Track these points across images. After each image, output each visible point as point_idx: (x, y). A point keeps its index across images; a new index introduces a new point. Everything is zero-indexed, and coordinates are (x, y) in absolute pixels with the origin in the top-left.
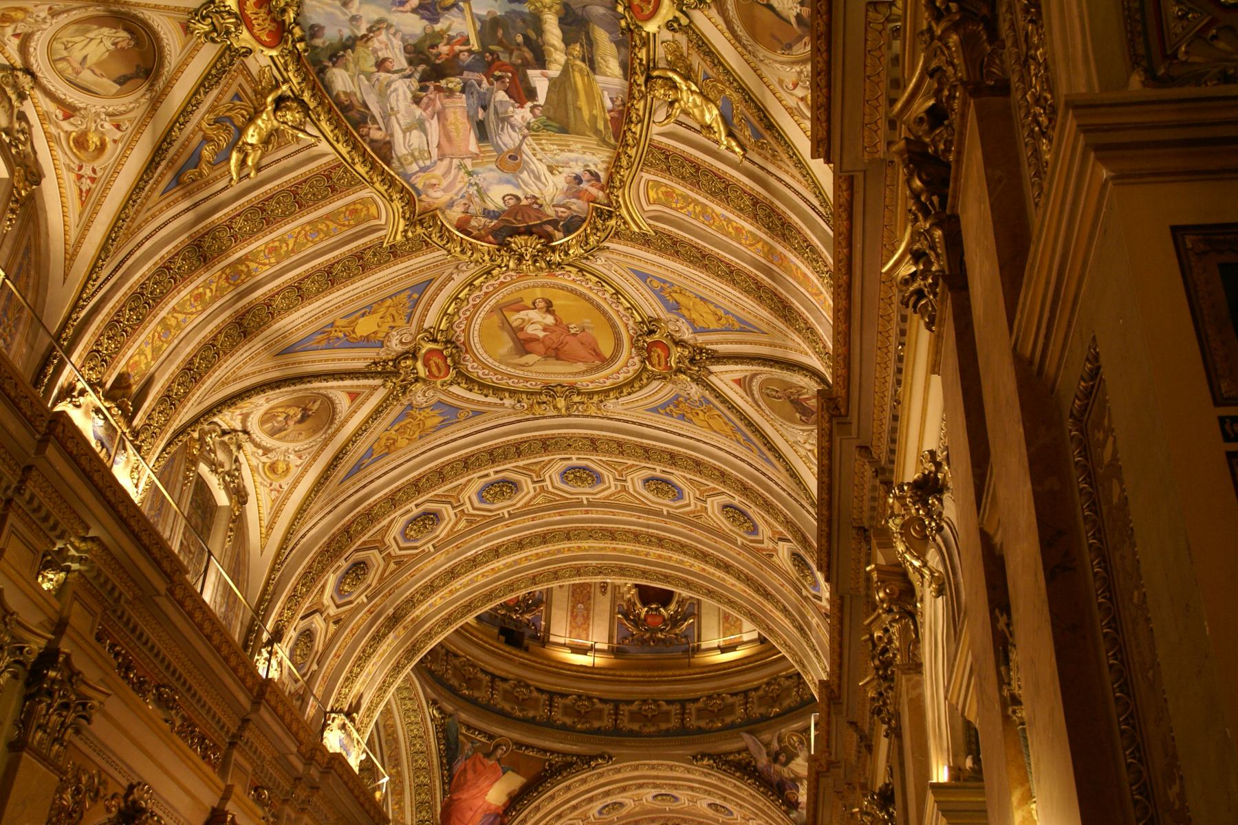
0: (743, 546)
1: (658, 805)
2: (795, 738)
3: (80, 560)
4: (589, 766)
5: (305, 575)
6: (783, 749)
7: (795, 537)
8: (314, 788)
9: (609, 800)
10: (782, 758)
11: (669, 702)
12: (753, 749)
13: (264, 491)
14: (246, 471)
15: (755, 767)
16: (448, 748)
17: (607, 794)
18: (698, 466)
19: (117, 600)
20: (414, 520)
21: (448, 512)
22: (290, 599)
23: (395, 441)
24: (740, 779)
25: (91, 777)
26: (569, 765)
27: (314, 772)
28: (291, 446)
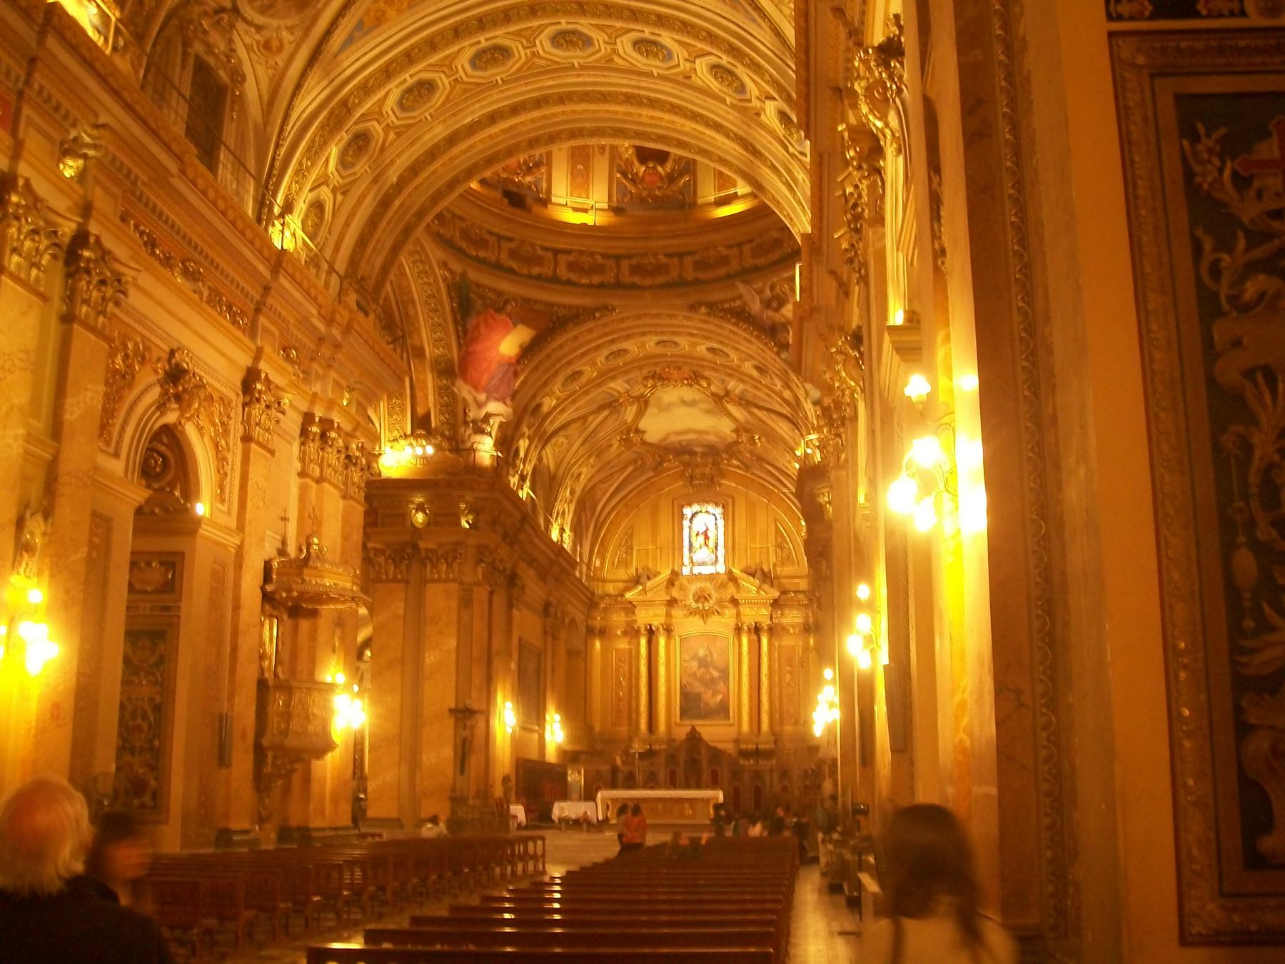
0: (733, 106)
1: (660, 350)
3: (95, 147)
4: (595, 318)
5: (309, 149)
6: (775, 297)
7: (781, 97)
8: (337, 346)
9: (615, 348)
10: (774, 304)
11: (668, 255)
12: (746, 297)
13: (261, 70)
14: (242, 52)
15: (749, 314)
16: (461, 305)
17: (613, 342)
18: (686, 27)
19: (134, 183)
20: (409, 91)
21: (443, 81)
22: (297, 172)
23: (384, 13)
24: (736, 325)
25: (136, 344)
26: (577, 316)
27: (336, 332)
28: (283, 23)
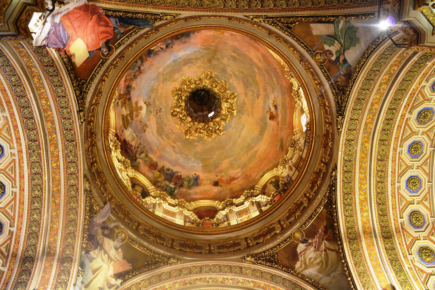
2: (123, 235)
6: (112, 231)
10: (106, 232)
